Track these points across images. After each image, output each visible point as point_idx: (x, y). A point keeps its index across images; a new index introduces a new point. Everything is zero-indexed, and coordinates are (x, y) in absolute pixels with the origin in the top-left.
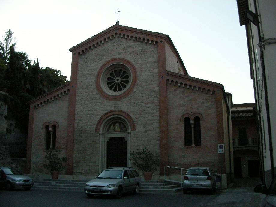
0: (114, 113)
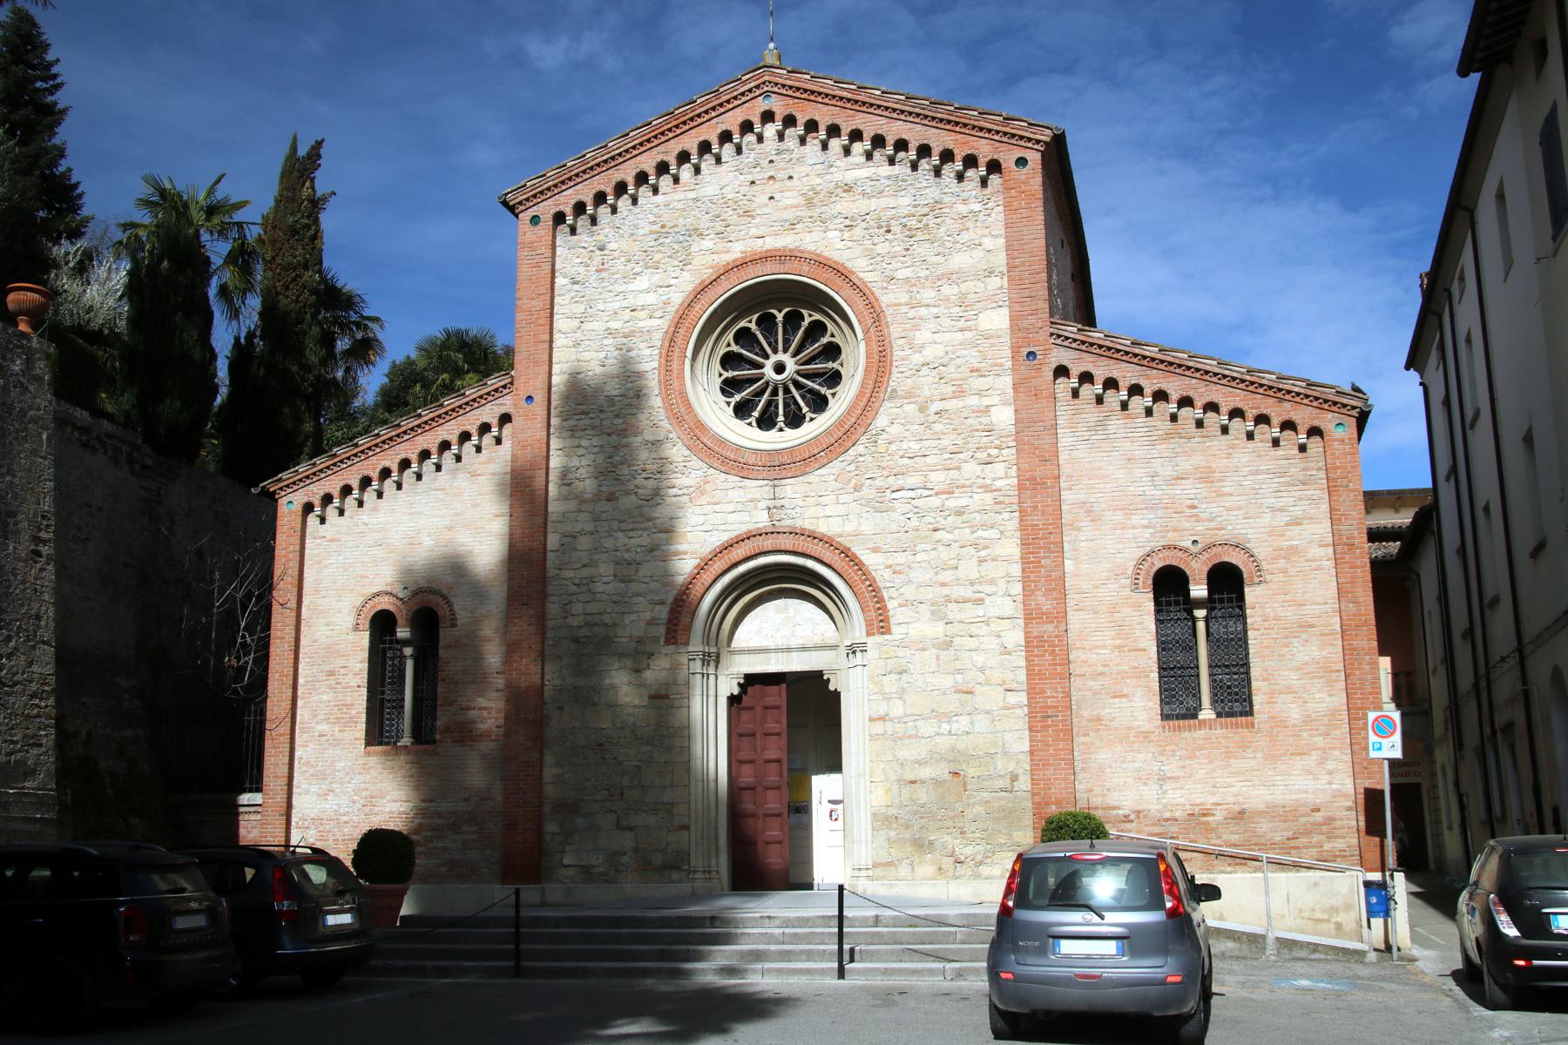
0: (768, 543)
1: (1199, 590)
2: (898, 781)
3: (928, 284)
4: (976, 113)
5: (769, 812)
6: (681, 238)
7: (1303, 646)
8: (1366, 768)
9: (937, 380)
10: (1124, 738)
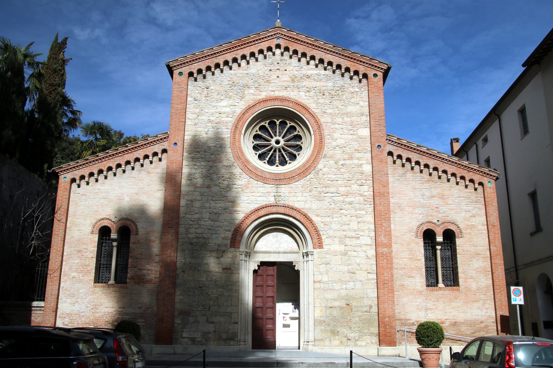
0: (274, 210)
1: (440, 239)
2: (326, 307)
3: (339, 116)
4: (359, 55)
5: (268, 317)
6: (241, 88)
7: (477, 261)
8: (500, 307)
9: (342, 152)
10: (412, 293)
